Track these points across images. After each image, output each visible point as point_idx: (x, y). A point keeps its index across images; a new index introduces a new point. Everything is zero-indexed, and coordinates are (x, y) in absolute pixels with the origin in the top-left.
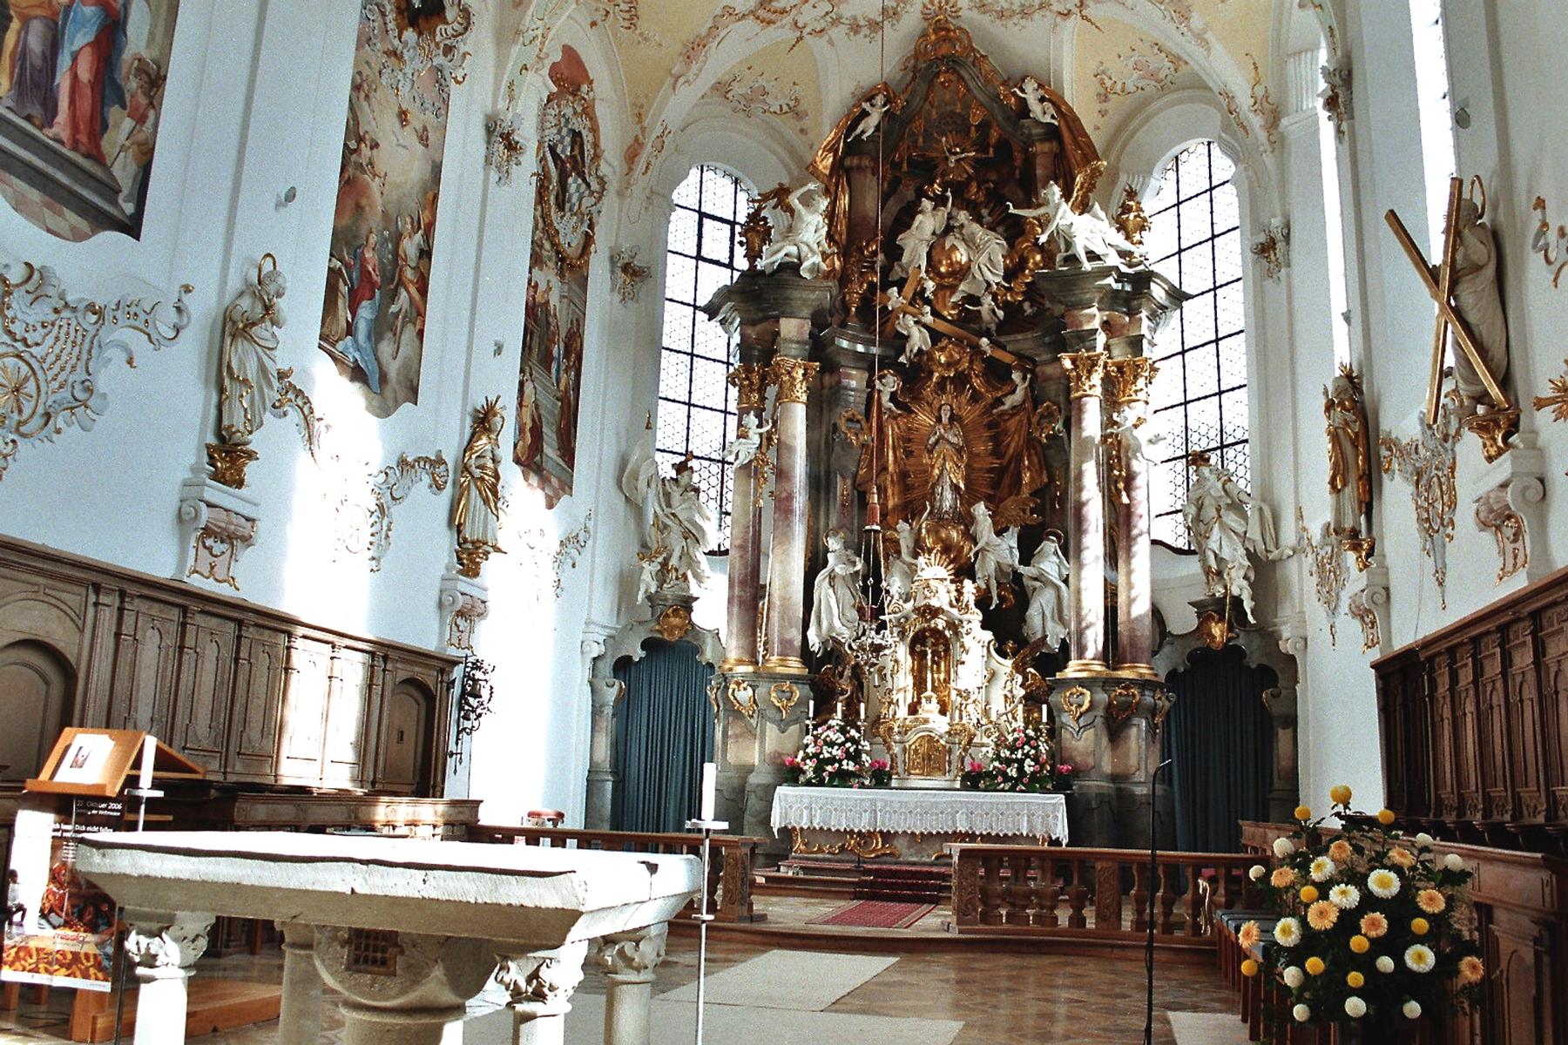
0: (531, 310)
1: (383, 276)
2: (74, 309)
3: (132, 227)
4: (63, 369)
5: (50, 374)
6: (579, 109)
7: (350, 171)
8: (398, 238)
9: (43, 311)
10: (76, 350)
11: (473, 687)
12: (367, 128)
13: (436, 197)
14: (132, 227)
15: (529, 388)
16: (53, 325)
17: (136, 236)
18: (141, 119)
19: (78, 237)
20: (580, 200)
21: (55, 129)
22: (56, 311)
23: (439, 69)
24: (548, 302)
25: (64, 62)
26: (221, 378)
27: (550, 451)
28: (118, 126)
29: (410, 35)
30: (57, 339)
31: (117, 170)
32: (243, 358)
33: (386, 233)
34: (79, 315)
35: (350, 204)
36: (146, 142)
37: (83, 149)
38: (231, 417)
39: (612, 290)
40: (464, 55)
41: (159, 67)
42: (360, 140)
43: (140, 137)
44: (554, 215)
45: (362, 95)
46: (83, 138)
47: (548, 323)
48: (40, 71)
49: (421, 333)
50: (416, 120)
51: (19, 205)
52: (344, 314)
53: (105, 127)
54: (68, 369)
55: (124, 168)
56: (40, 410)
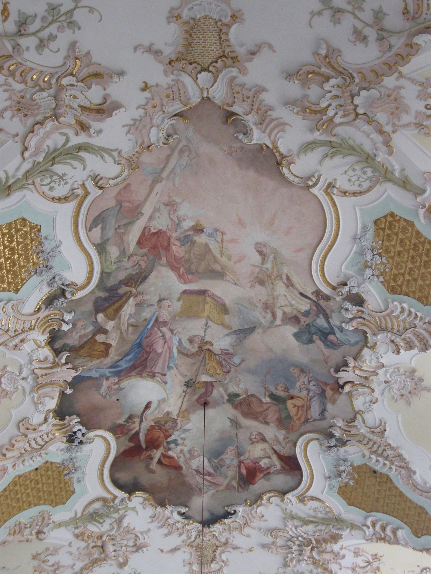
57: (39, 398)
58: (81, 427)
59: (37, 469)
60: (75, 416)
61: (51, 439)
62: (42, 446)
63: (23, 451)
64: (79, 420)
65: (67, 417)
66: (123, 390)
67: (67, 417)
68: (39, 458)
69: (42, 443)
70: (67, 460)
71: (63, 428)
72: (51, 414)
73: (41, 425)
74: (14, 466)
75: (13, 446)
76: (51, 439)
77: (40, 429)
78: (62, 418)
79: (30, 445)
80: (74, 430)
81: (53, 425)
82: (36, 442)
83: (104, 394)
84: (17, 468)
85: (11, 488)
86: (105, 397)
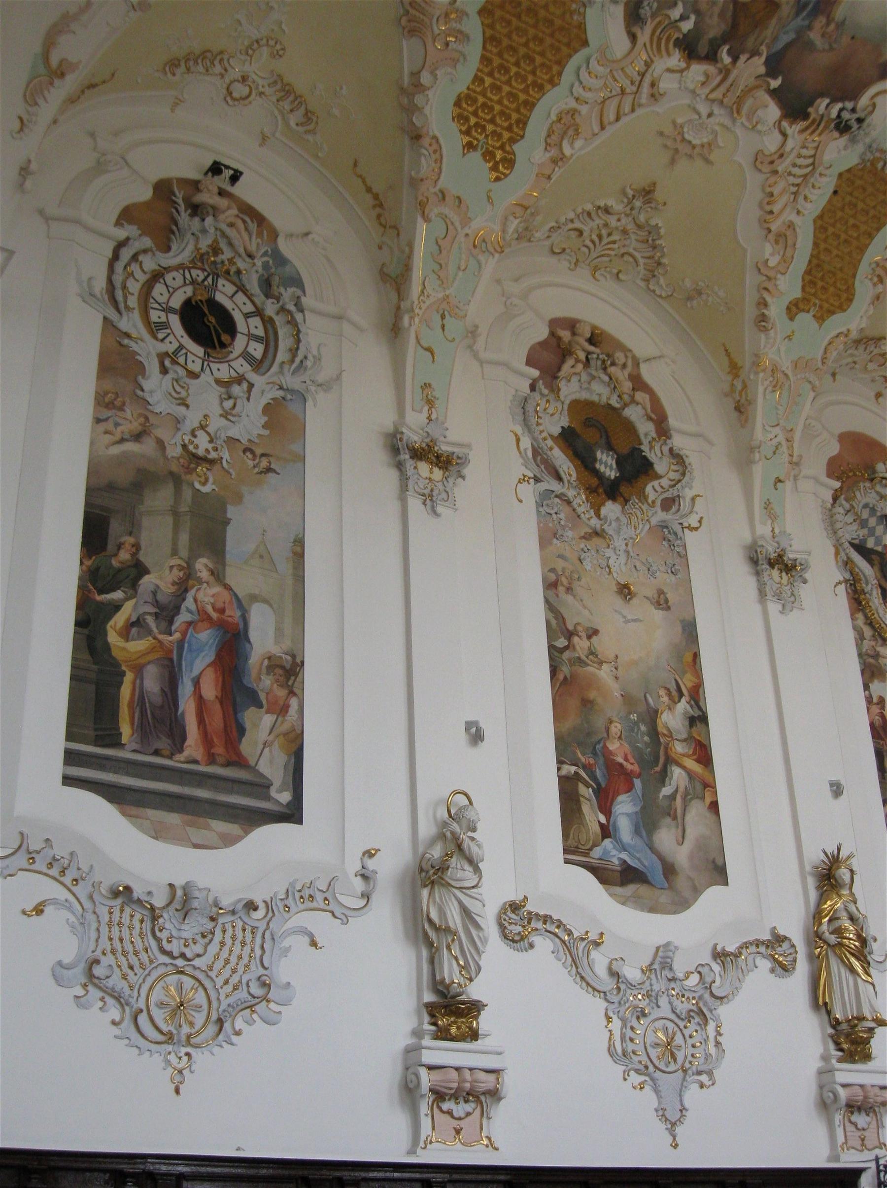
1: (641, 761)
2: (233, 912)
3: (292, 814)
4: (234, 971)
5: (219, 981)
7: (565, 670)
8: (652, 716)
9: (192, 928)
10: (247, 949)
13: (696, 656)
14: (292, 814)
16: (213, 933)
17: (300, 821)
18: (284, 710)
19: (229, 841)
21: (187, 753)
22: (212, 919)
23: (663, 526)
25: (186, 689)
26: (428, 936)
28: (256, 726)
30: (223, 943)
31: (264, 767)
33: (634, 717)
34: (242, 914)
35: (573, 703)
37: (220, 760)
41: (294, 657)
43: (286, 727)
45: (561, 589)
46: (219, 750)
48: (162, 707)
49: (714, 807)
50: (644, 587)
51: (158, 833)
52: (592, 817)
54: (241, 969)
56: (214, 1017)
59: (835, 192)
60: (819, 100)
61: (817, 148)
62: (813, 164)
63: (794, 189)
64: (827, 101)
65: (810, 110)
66: (847, 22)
67: (810, 110)
68: (824, 180)
69: (810, 161)
71: (819, 125)
72: (785, 124)
73: (783, 145)
74: (798, 212)
76: (817, 148)
78: (806, 116)
79: (794, 176)
81: (802, 131)
83: (827, 47)
84: (806, 212)
85: (822, 236)
86: (831, 49)
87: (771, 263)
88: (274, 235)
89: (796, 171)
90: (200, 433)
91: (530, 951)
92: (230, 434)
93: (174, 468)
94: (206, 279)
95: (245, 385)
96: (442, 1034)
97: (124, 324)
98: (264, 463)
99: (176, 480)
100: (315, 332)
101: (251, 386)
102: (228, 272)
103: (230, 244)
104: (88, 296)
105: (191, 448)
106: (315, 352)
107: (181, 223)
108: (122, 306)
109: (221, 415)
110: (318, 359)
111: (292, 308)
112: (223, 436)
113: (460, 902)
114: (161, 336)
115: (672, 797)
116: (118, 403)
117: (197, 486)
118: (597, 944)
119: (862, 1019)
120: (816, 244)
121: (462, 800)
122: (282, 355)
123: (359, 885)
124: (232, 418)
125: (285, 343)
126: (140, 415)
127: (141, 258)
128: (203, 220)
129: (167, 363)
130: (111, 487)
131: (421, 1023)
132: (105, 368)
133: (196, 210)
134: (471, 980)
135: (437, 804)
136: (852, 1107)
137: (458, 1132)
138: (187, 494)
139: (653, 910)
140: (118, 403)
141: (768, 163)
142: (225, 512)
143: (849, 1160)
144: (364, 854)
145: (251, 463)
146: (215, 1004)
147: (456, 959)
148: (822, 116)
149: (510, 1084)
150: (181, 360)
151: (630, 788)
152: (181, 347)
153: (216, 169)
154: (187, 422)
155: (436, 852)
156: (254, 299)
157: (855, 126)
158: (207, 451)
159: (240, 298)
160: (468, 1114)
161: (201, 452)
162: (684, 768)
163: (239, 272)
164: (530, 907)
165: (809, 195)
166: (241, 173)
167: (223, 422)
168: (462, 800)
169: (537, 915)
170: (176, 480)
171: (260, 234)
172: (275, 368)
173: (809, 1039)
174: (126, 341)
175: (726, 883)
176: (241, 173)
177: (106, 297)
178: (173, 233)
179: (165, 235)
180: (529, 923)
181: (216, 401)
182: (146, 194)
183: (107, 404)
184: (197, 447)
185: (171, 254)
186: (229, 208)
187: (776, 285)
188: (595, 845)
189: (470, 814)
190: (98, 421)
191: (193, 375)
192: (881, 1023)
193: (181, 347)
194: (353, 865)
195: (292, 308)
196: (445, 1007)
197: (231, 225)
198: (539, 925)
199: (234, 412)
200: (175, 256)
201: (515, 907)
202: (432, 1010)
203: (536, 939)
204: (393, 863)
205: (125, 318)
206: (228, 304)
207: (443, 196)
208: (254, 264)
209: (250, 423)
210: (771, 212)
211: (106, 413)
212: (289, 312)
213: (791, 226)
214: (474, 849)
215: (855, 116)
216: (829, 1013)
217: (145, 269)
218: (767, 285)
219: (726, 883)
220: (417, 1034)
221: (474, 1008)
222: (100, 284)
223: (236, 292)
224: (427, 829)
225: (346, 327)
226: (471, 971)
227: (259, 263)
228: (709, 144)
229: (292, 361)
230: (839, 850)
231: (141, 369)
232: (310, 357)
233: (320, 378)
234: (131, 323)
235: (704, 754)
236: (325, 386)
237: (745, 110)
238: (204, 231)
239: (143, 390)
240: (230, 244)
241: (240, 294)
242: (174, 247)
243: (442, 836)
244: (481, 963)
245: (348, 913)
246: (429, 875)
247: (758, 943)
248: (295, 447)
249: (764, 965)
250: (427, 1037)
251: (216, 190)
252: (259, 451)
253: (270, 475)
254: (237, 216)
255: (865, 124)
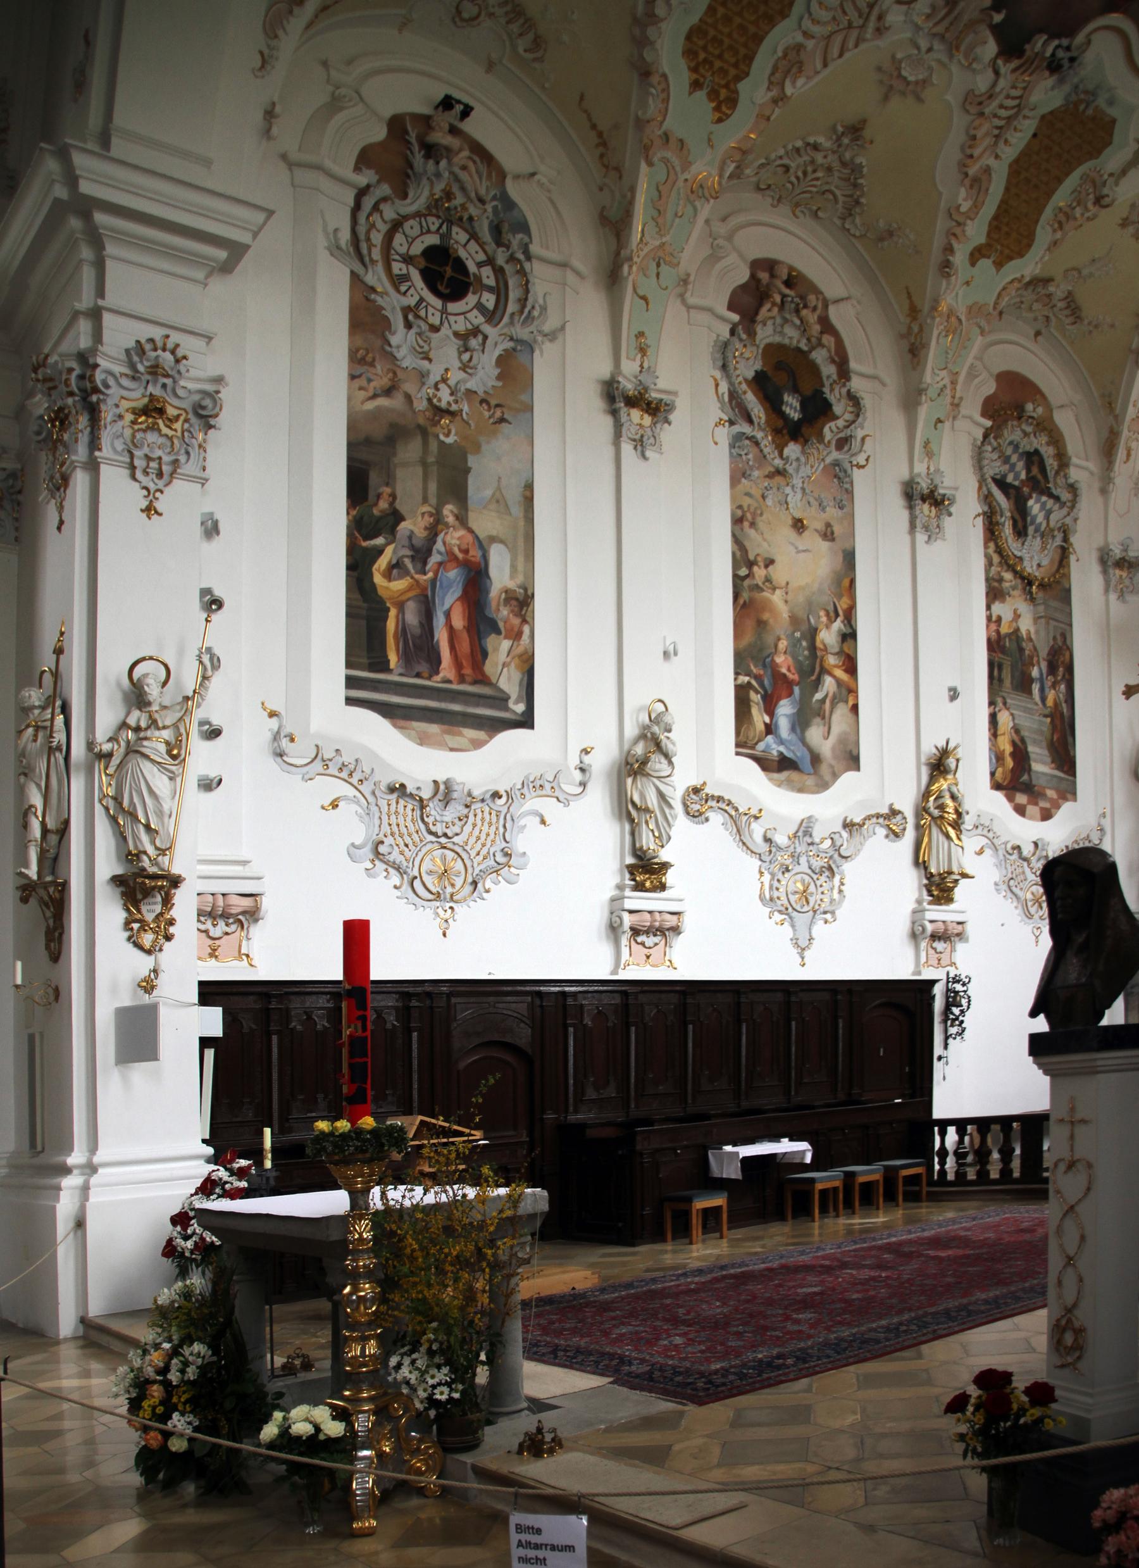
0: (995, 645)
2: (483, 801)
3: (526, 721)
4: (484, 845)
5: (473, 853)
6: (1029, 429)
7: (745, 595)
8: (813, 633)
9: (450, 814)
10: (493, 828)
11: (954, 998)
12: (757, 551)
13: (852, 582)
14: (526, 721)
15: (1004, 718)
16: (467, 817)
17: (532, 727)
18: (518, 635)
19: (477, 745)
20: (1047, 518)
21: (441, 675)
22: (467, 806)
24: (1017, 630)
25: (439, 621)
26: (629, 812)
27: (1041, 767)
28: (496, 649)
29: (792, 450)
30: (475, 825)
31: (503, 684)
32: (644, 792)
33: (798, 634)
34: (489, 801)
35: (750, 624)
36: (526, 652)
37: (468, 679)
38: (641, 840)
39: (1107, 590)
40: (863, 439)
41: (526, 590)
42: (751, 564)
43: (520, 650)
44: (1013, 545)
45: (746, 524)
46: (468, 671)
47: (1021, 650)
48: (421, 636)
49: (855, 709)
50: (814, 521)
51: (423, 740)
52: (759, 718)
53: (485, 654)
54: (489, 843)
55: (509, 679)
56: (470, 879)
57: (966, 56)
58: (1056, 42)
59: (1035, 135)
62: (1019, 105)
63: (996, 132)
64: (1045, 37)
65: (1027, 47)
67: (1027, 47)
68: (1027, 122)
69: (1016, 102)
70: (1069, 94)
71: (1032, 63)
72: (1000, 62)
75: (974, 138)
76: (1025, 89)
77: (998, 89)
78: (1020, 53)
80: (1048, 54)
81: (1014, 70)
82: (1006, 108)
84: (1003, 156)
87: (963, 209)
88: (502, 175)
89: (1003, 113)
90: (442, 386)
91: (706, 824)
92: (469, 385)
93: (421, 421)
94: (440, 227)
95: (480, 338)
96: (639, 887)
97: (370, 279)
98: (498, 414)
99: (424, 432)
100: (542, 279)
101: (486, 337)
102: (461, 219)
103: (463, 189)
104: (335, 249)
105: (435, 401)
106: (541, 301)
107: (416, 165)
108: (367, 259)
109: (460, 368)
110: (544, 309)
111: (521, 257)
112: (463, 389)
113: (657, 789)
114: (403, 288)
115: (823, 701)
116: (369, 358)
117: (442, 437)
118: (756, 818)
119: (950, 873)
120: (1007, 189)
121: (660, 707)
122: (512, 307)
123: (578, 776)
124: (469, 371)
125: (514, 294)
126: (389, 370)
127: (382, 207)
128: (438, 163)
129: (411, 317)
130: (368, 442)
131: (623, 879)
132: (356, 325)
133: (431, 151)
134: (662, 846)
135: (640, 709)
136: (935, 937)
137: (648, 957)
138: (434, 446)
139: (801, 790)
140: (369, 358)
141: (974, 103)
142: (466, 461)
143: (927, 974)
144: (581, 751)
145: (487, 414)
146: (470, 870)
147: (652, 831)
148: (1037, 54)
149: (688, 923)
150: (422, 313)
151: (790, 694)
152: (422, 300)
153: (447, 103)
154: (431, 376)
155: (639, 749)
156: (487, 248)
157: (1066, 63)
158: (449, 403)
159: (473, 246)
160: (656, 944)
161: (443, 405)
162: (834, 676)
163: (471, 219)
164: (708, 790)
165: (1010, 139)
166: (472, 109)
167: (462, 375)
168: (660, 707)
169: (713, 796)
170: (424, 432)
171: (489, 176)
172: (506, 319)
173: (908, 886)
174: (373, 296)
175: (858, 769)
176: (472, 109)
177: (351, 249)
178: (408, 176)
179: (402, 180)
180: (706, 801)
181: (456, 354)
182: (380, 134)
183: (359, 361)
184: (440, 400)
185: (408, 201)
186: (461, 150)
187: (964, 231)
188: (760, 740)
189: (667, 719)
190: (352, 377)
191: (435, 329)
192: (964, 876)
193: (422, 300)
194: (574, 760)
195: (521, 257)
196: (642, 867)
197: (464, 168)
198: (713, 803)
199: (471, 364)
200: (412, 203)
201: (696, 790)
202: (632, 870)
203: (710, 814)
204: (604, 758)
205: (370, 270)
206: (462, 254)
207: (666, 137)
208: (485, 210)
209: (485, 377)
210: (971, 156)
211: (360, 370)
212: (519, 261)
213: (987, 170)
214: (670, 746)
215: (1069, 54)
216: (926, 868)
217: (386, 218)
218: (958, 231)
219: (858, 769)
220: (620, 887)
221: (665, 866)
222: (345, 236)
223: (469, 241)
224: (631, 731)
225: (571, 277)
226: (662, 839)
227: (489, 208)
228: (924, 81)
229: (522, 312)
230: (947, 743)
231: (386, 324)
232: (537, 308)
233: (546, 328)
234: (376, 277)
235: (851, 666)
236: (552, 336)
237: (963, 48)
238: (438, 175)
239: (390, 345)
240: (463, 189)
241: (472, 242)
242: (411, 194)
243: (643, 736)
244: (671, 834)
245: (569, 798)
246: (633, 767)
247: (878, 816)
248: (524, 397)
249: (882, 832)
250: (627, 890)
251: (447, 127)
252: (493, 402)
253: (504, 424)
254: (470, 158)
255: (1076, 64)
